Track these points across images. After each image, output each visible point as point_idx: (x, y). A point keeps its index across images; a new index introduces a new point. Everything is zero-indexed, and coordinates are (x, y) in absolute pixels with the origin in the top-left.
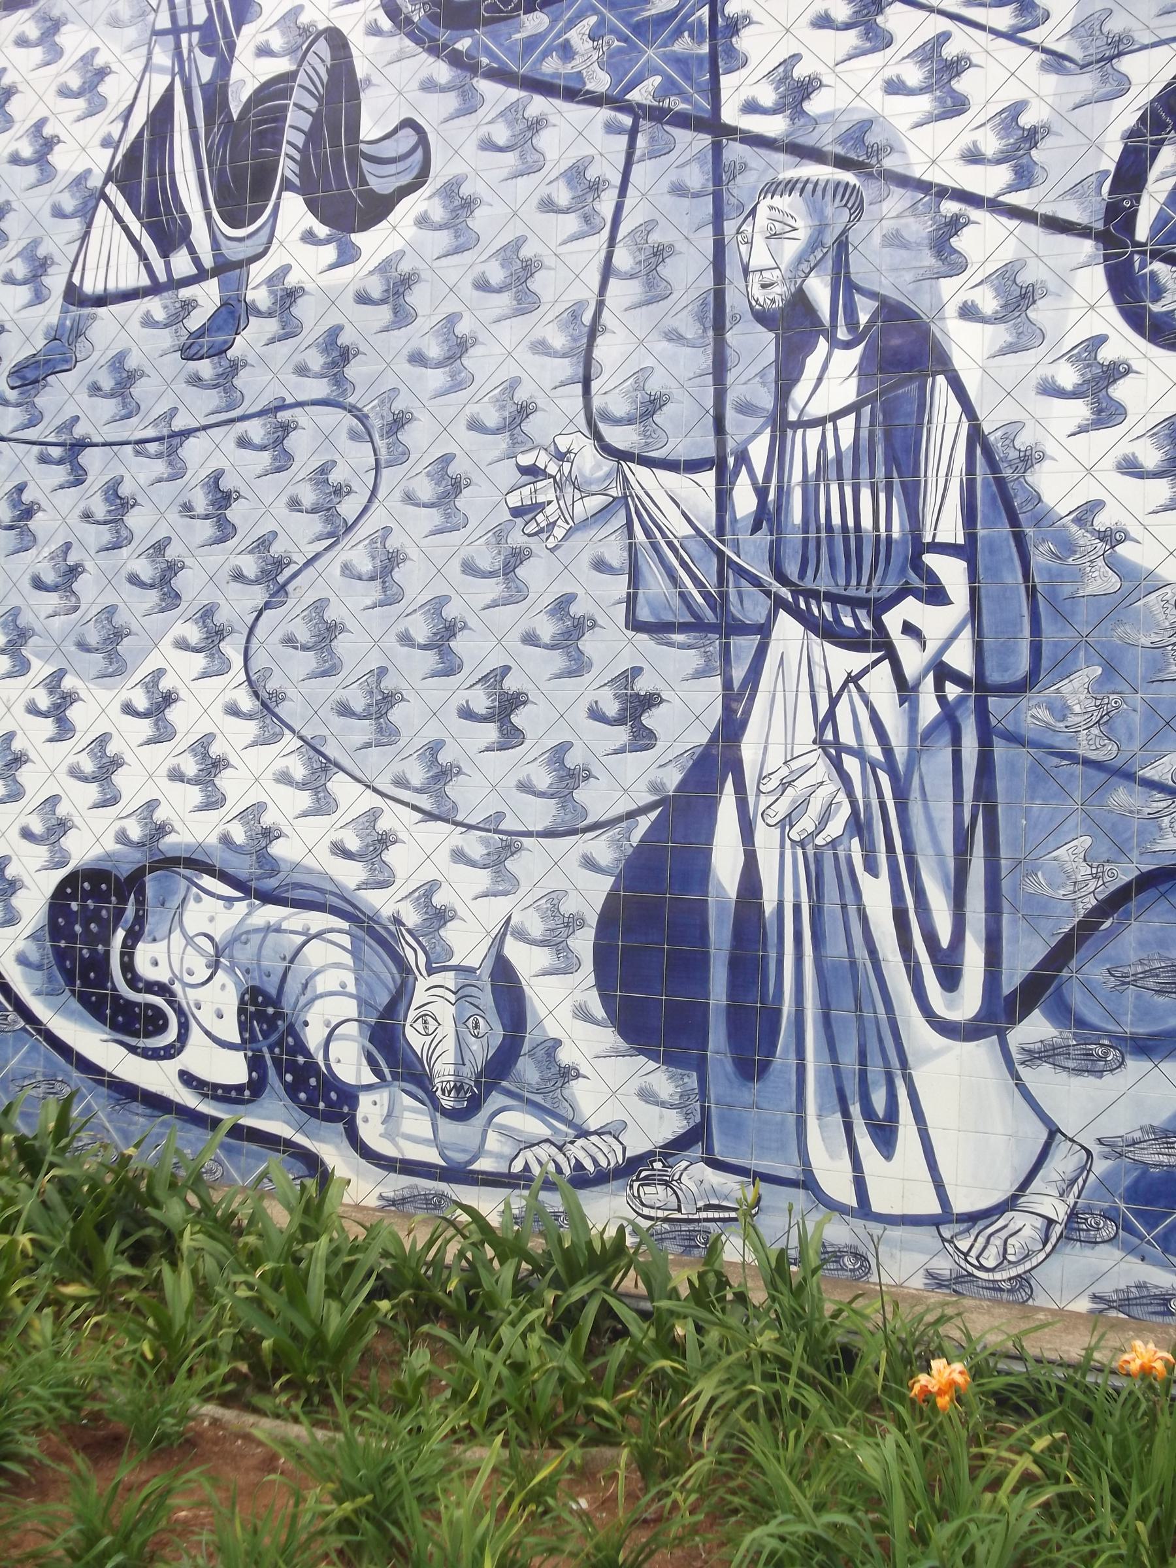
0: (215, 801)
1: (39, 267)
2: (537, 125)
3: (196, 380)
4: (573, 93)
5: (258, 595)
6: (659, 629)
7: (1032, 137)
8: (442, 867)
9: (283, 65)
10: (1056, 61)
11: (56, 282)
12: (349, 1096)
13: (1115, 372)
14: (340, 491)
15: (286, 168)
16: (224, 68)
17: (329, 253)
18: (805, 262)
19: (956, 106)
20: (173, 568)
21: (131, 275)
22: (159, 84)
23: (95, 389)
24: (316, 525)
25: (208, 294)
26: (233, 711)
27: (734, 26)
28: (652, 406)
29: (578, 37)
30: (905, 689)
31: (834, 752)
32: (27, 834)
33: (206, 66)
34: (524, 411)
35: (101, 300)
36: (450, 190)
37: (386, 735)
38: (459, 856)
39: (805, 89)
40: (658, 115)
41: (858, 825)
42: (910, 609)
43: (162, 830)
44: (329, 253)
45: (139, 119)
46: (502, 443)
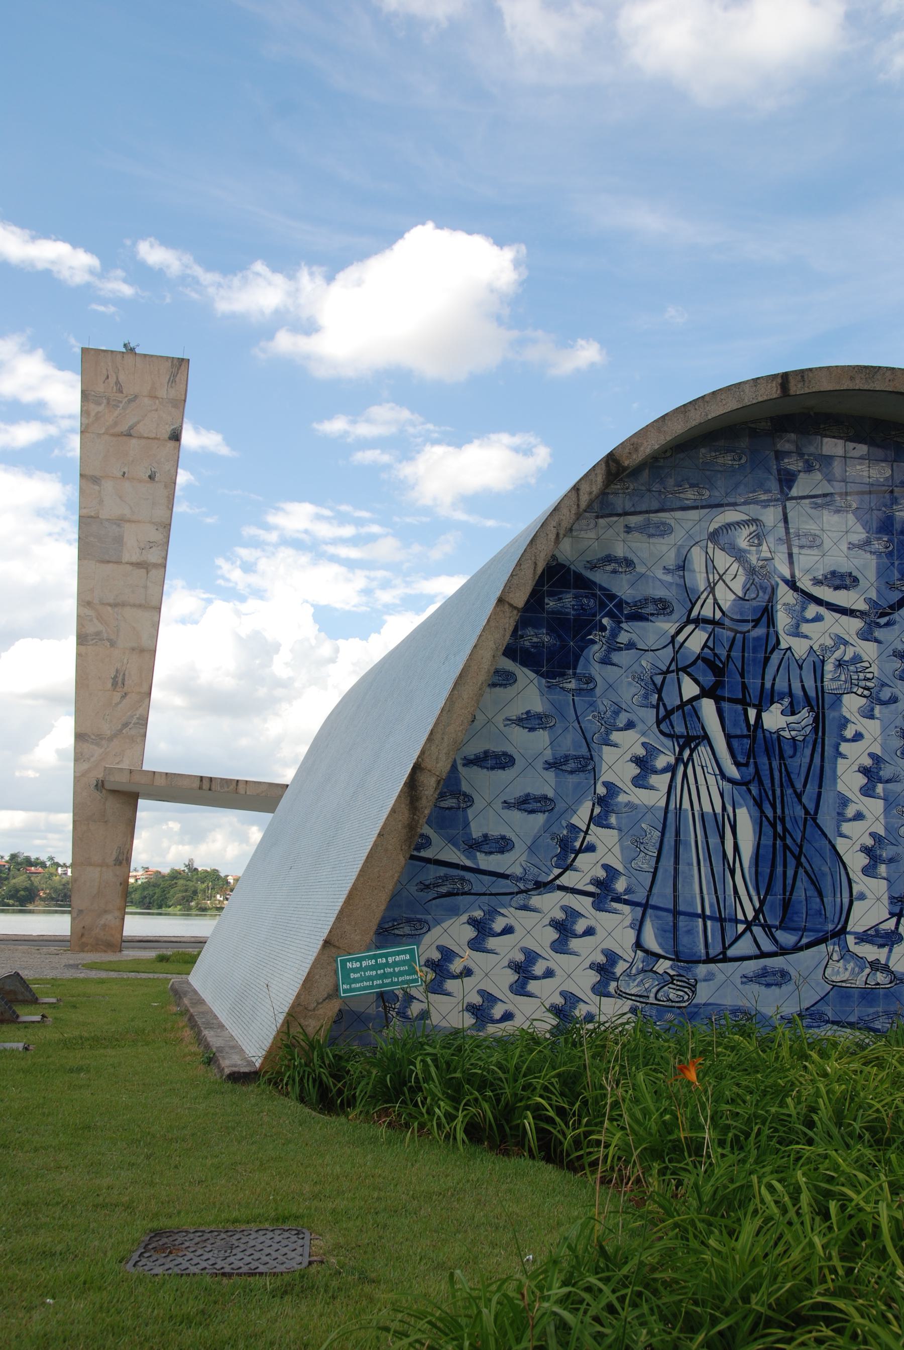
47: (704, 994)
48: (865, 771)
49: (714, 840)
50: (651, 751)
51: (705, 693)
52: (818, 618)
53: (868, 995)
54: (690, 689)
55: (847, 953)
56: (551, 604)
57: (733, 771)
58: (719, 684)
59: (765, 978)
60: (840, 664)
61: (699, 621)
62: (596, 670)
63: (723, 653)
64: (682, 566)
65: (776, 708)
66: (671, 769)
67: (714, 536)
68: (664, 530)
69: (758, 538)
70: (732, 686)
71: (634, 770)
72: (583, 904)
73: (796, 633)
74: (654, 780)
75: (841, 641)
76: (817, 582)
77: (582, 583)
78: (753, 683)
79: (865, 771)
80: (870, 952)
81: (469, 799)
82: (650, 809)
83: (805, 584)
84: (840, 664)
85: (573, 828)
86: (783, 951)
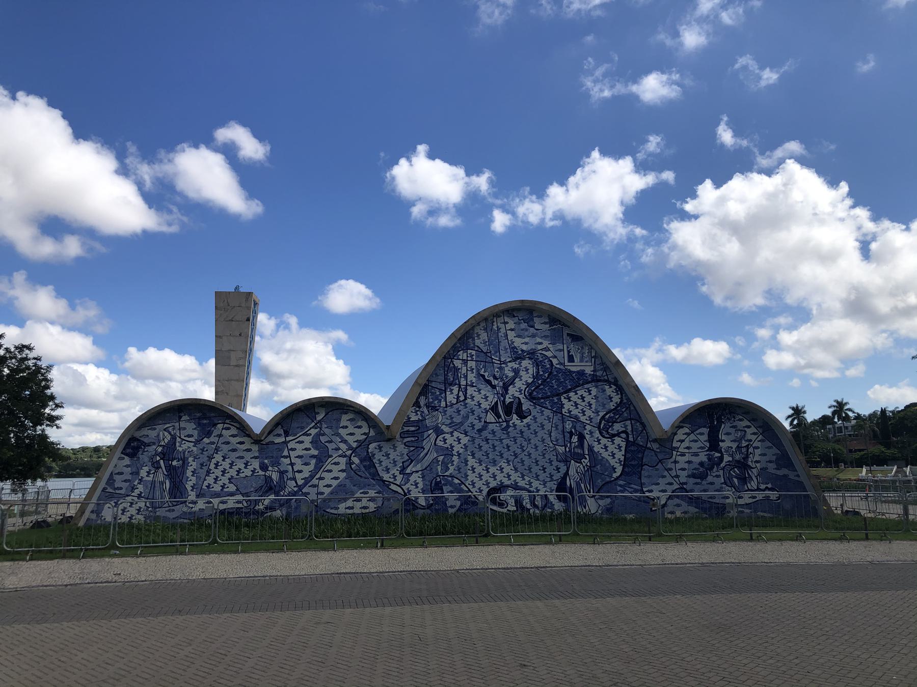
0: (510, 479)
1: (480, 419)
2: (543, 411)
3: (504, 433)
4: (547, 408)
5: (514, 457)
6: (559, 461)
7: (592, 418)
8: (538, 485)
9: (512, 400)
10: (593, 412)
11: (483, 420)
12: (529, 510)
13: (600, 440)
14: (523, 447)
15: (513, 411)
16: (505, 399)
17: (520, 421)
18: (571, 428)
19: (585, 415)
20: (502, 454)
21: (494, 421)
22: (496, 400)
23: (490, 433)
24: (521, 450)
25: (505, 424)
26: (511, 469)
27: (564, 404)
28: (557, 440)
29: (547, 403)
30: (584, 467)
31: (577, 473)
32: (483, 484)
33: (502, 399)
34: (544, 440)
35: (490, 423)
36: (534, 416)
37: (531, 472)
38: (540, 484)
39: (571, 411)
40: (556, 412)
41: (580, 479)
42: (584, 460)
43: (503, 483)
44: (520, 421)
45: (493, 403)
46: (542, 443)
47: (158, 514)
48: (192, 472)
49: (161, 486)
50: (150, 470)
51: (161, 459)
52: (185, 443)
53: (190, 513)
54: (158, 458)
55: (186, 506)
56: (132, 444)
57: (166, 473)
58: (164, 457)
59: (169, 511)
60: (189, 452)
61: (161, 446)
62: (140, 456)
63: (165, 451)
64: (158, 435)
65: (175, 461)
66: (154, 473)
67: (165, 430)
68: (155, 429)
69: (174, 429)
70: (167, 456)
71: (147, 474)
72: (136, 499)
73: (180, 446)
74: (150, 475)
75: (189, 447)
76: (185, 436)
77: (138, 440)
78: (171, 457)
79: (192, 472)
80: (191, 505)
81: (115, 480)
82: (149, 481)
83: (182, 437)
84: (189, 452)
85: (134, 485)
86: (174, 506)
